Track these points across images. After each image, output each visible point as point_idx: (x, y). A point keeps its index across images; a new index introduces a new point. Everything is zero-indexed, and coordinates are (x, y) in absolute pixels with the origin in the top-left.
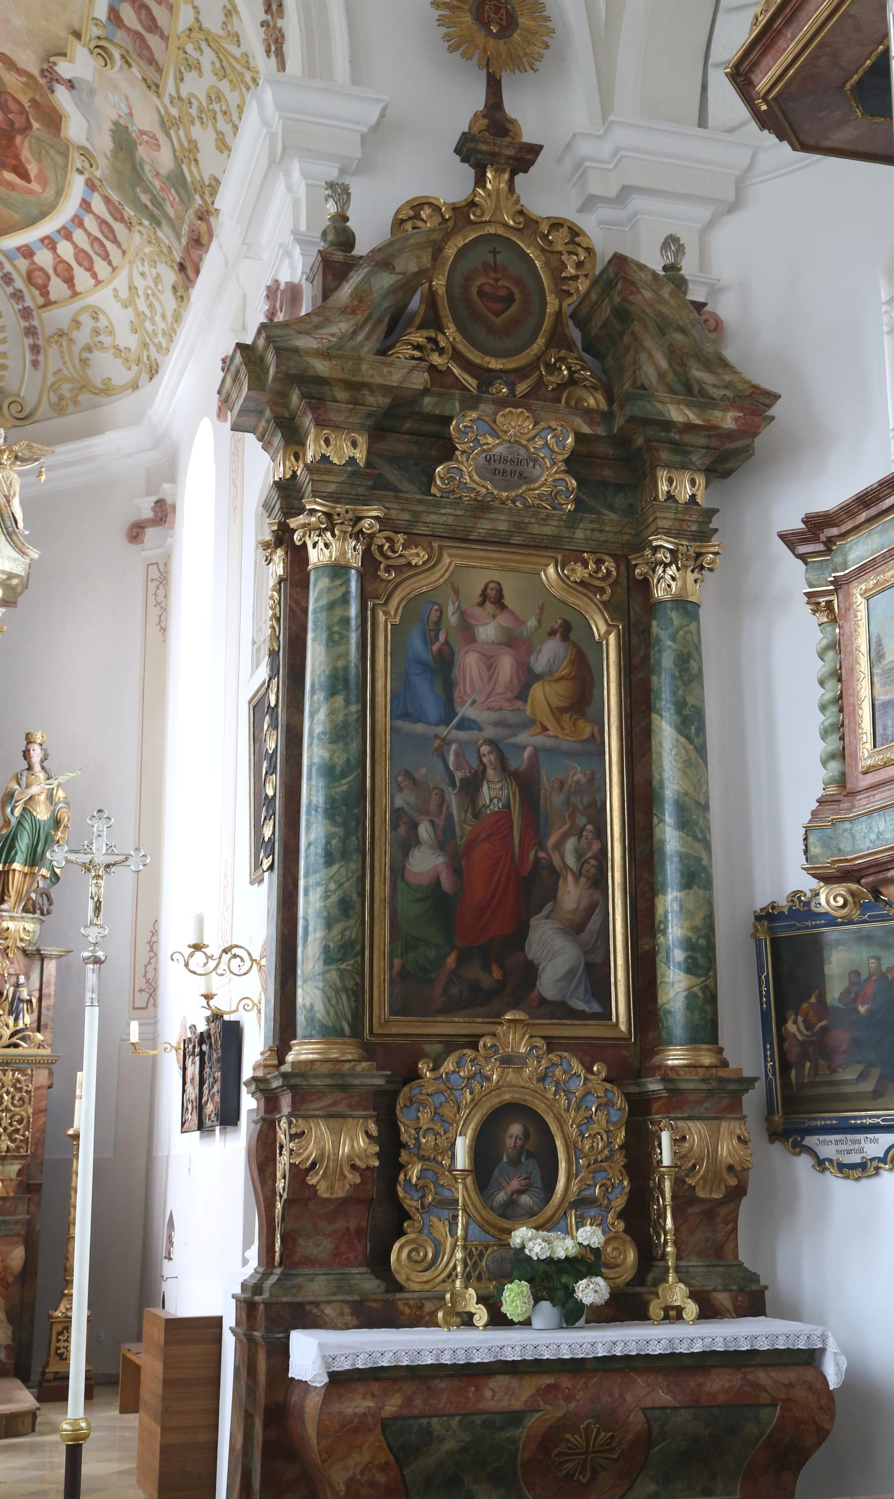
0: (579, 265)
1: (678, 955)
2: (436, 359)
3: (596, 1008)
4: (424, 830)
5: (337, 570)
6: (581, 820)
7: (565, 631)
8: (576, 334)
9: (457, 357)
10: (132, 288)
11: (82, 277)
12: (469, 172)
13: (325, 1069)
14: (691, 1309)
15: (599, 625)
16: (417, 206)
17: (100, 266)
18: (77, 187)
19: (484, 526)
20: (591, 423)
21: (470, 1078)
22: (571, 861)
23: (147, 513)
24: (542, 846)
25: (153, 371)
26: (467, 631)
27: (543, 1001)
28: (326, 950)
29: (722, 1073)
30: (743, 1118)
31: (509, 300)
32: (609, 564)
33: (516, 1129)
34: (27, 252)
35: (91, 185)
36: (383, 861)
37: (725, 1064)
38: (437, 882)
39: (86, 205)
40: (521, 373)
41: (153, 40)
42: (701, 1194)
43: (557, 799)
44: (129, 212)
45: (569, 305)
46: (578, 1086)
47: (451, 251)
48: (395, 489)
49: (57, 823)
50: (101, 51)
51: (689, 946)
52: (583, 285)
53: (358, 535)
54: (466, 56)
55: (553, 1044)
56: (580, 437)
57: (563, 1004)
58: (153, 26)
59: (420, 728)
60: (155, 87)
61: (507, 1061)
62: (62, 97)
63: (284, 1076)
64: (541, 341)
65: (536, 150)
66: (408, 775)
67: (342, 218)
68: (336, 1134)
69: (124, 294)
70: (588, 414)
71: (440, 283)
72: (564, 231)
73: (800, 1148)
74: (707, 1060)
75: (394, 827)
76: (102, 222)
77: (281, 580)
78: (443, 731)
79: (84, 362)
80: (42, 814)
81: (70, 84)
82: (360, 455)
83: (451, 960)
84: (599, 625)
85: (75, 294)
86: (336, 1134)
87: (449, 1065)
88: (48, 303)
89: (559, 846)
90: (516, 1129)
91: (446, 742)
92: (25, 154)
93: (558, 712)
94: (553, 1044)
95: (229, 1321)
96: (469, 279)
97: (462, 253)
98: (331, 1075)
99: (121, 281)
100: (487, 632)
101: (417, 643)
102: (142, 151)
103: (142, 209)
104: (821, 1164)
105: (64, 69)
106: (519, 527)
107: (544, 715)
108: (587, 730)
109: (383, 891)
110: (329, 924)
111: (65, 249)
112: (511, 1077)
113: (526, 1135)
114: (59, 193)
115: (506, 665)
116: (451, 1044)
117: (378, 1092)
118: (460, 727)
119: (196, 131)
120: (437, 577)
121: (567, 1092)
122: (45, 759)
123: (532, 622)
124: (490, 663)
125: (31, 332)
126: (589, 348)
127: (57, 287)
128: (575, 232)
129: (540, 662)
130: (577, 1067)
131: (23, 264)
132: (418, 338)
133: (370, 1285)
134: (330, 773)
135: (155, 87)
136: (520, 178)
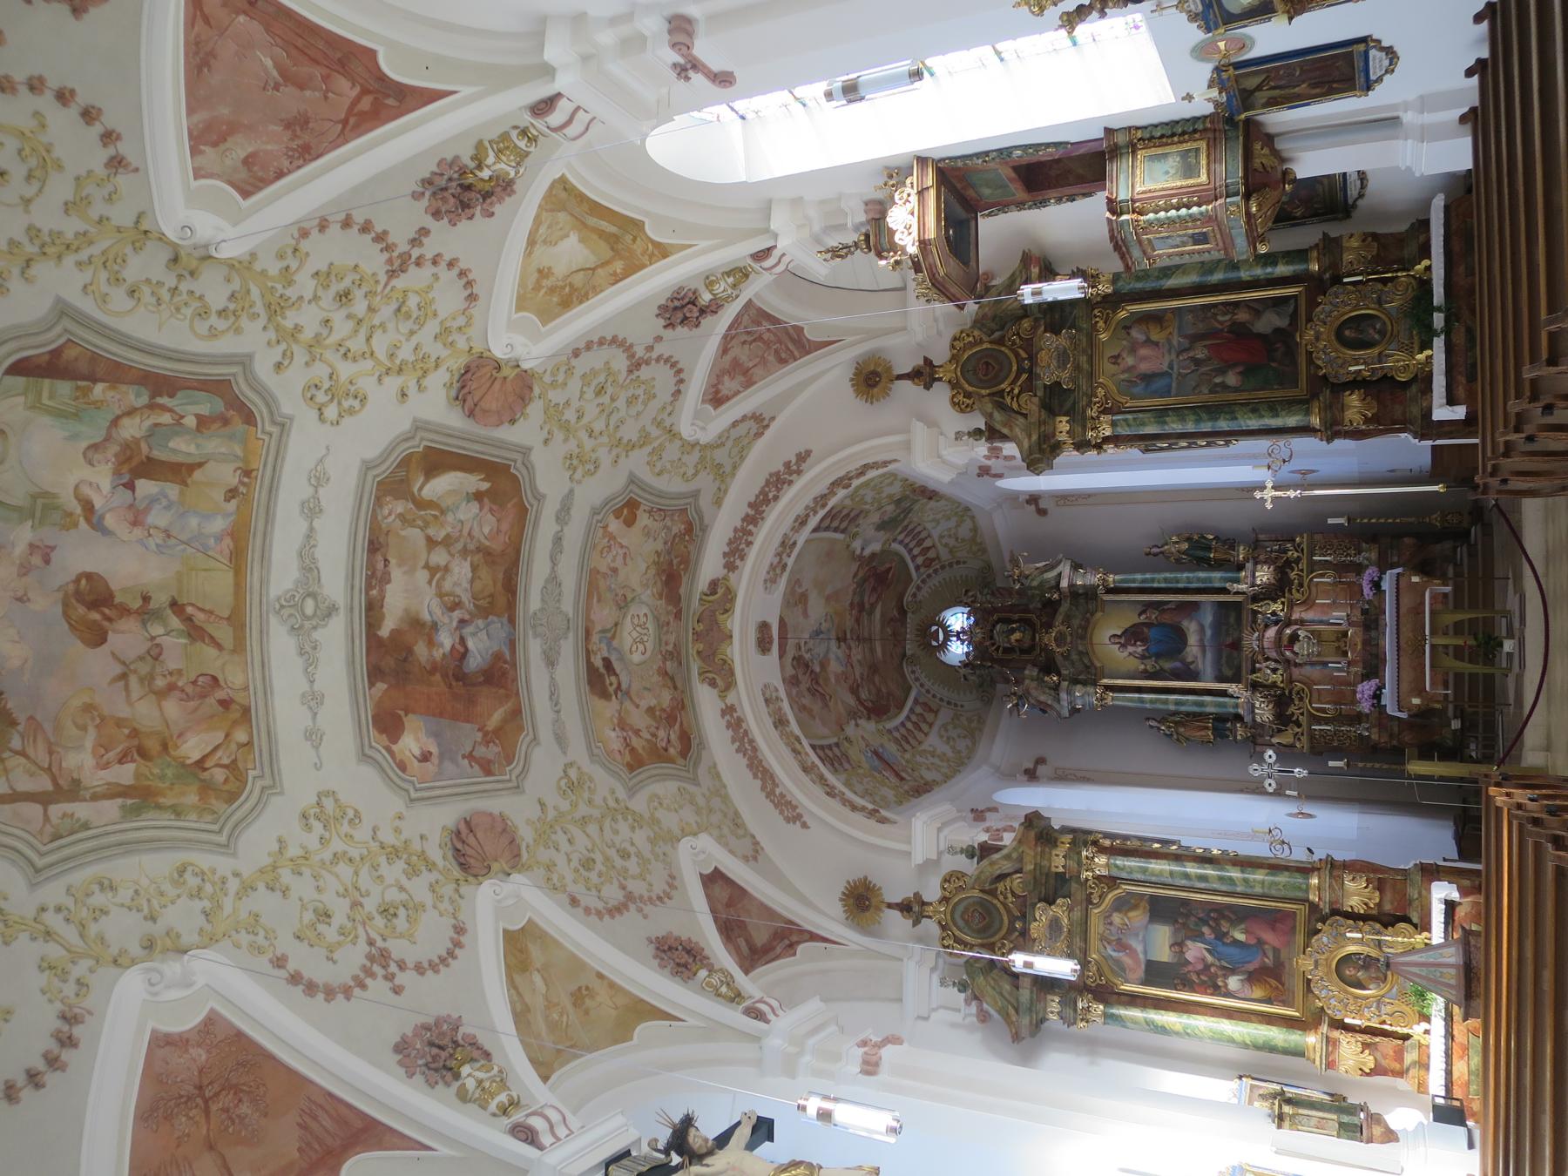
0: (968, 335)
1: (1269, 270)
2: (1016, 391)
3: (1292, 301)
4: (1218, 380)
5: (1114, 424)
6: (1209, 314)
7: (1127, 328)
8: (997, 334)
9: (1014, 382)
10: (933, 520)
11: (928, 543)
12: (936, 384)
13: (1323, 414)
14: (1425, 263)
15: (1122, 314)
16: (954, 404)
17: (923, 535)
18: (896, 546)
19: (1086, 366)
20: (1040, 326)
21: (1325, 353)
22: (1227, 317)
23: (1033, 507)
24: (1222, 330)
25: (967, 509)
26: (1130, 369)
27: (1290, 325)
28: (1273, 417)
29: (1321, 246)
30: (1341, 237)
31: (987, 364)
32: (1096, 312)
33: (1347, 333)
34: (917, 568)
35: (895, 540)
36: (1232, 396)
37: (1317, 245)
38: (1240, 373)
39: (901, 542)
40: (1017, 355)
41: (852, 515)
42: (1374, 253)
43: (1201, 325)
44: (905, 523)
45: (985, 338)
46: (1328, 308)
47: (970, 389)
48: (1074, 403)
49: (1189, 539)
50: (854, 536)
51: (1265, 265)
52: (976, 333)
53: (1098, 418)
54: (890, 389)
55: (1309, 320)
56: (1045, 331)
57: (1291, 316)
58: (848, 515)
59: (1174, 385)
60: (868, 512)
61: (1317, 339)
62: (867, 552)
63: (1326, 429)
64: (1003, 349)
65: (926, 359)
66: (1194, 388)
67: (969, 434)
68: (1350, 407)
69: (934, 524)
70: (1034, 328)
71: (984, 392)
72: (957, 344)
73: (1354, 206)
74: (1315, 254)
75: (1216, 392)
76: (907, 536)
77: (1116, 446)
78: (1174, 376)
79: (963, 540)
80: (1185, 546)
81: (863, 549)
82: (1065, 419)
83: (1274, 365)
84: (1122, 314)
85: (934, 546)
86: (1350, 407)
87: (1319, 363)
88: (938, 558)
89: (1221, 323)
90: (1347, 333)
91: (1179, 374)
92: (883, 569)
93: (1162, 328)
94: (1309, 320)
95: (1430, 443)
96: (981, 380)
97: (970, 384)
98: (1325, 410)
99: (929, 526)
100: (1130, 361)
101: (1136, 390)
102: (886, 518)
103: (905, 517)
104: (1361, 196)
105: (858, 552)
106: (1084, 351)
107: (1163, 335)
108: (1169, 315)
109: (1245, 395)
110: (1262, 417)
111: (916, 551)
112: (1324, 336)
113: (1350, 328)
114: (897, 554)
115: (1143, 352)
116: (1310, 360)
117: (1332, 392)
118: (1172, 368)
119: (884, 495)
120: (1110, 384)
121: (1331, 312)
122: (1157, 546)
123: (1124, 343)
124: (1144, 359)
125: (951, 565)
126: (1002, 328)
127: (931, 554)
128: (955, 339)
129: (1142, 338)
130: (1319, 309)
131: (922, 570)
132: (1008, 400)
133: (1414, 388)
134: (1198, 421)
135: (868, 512)
136: (935, 363)
